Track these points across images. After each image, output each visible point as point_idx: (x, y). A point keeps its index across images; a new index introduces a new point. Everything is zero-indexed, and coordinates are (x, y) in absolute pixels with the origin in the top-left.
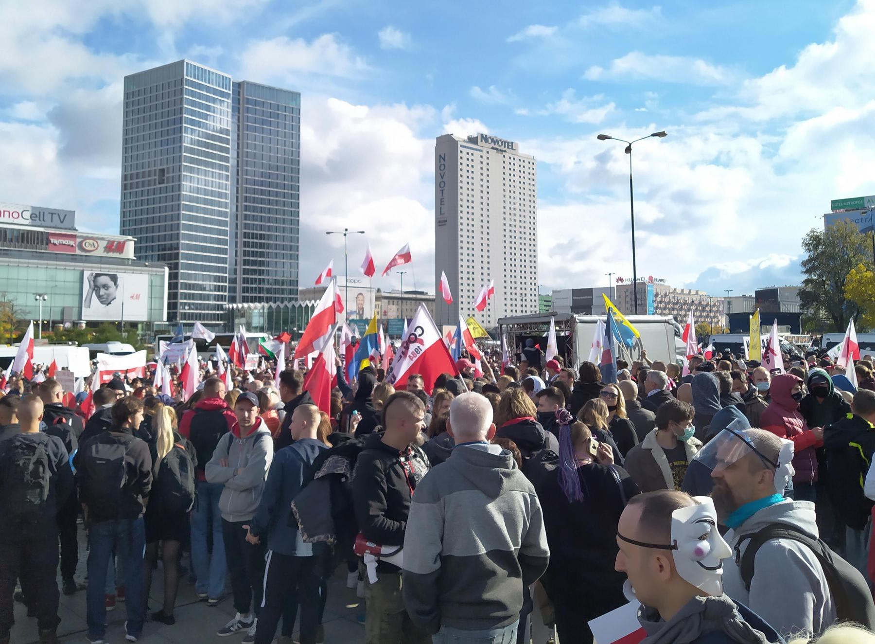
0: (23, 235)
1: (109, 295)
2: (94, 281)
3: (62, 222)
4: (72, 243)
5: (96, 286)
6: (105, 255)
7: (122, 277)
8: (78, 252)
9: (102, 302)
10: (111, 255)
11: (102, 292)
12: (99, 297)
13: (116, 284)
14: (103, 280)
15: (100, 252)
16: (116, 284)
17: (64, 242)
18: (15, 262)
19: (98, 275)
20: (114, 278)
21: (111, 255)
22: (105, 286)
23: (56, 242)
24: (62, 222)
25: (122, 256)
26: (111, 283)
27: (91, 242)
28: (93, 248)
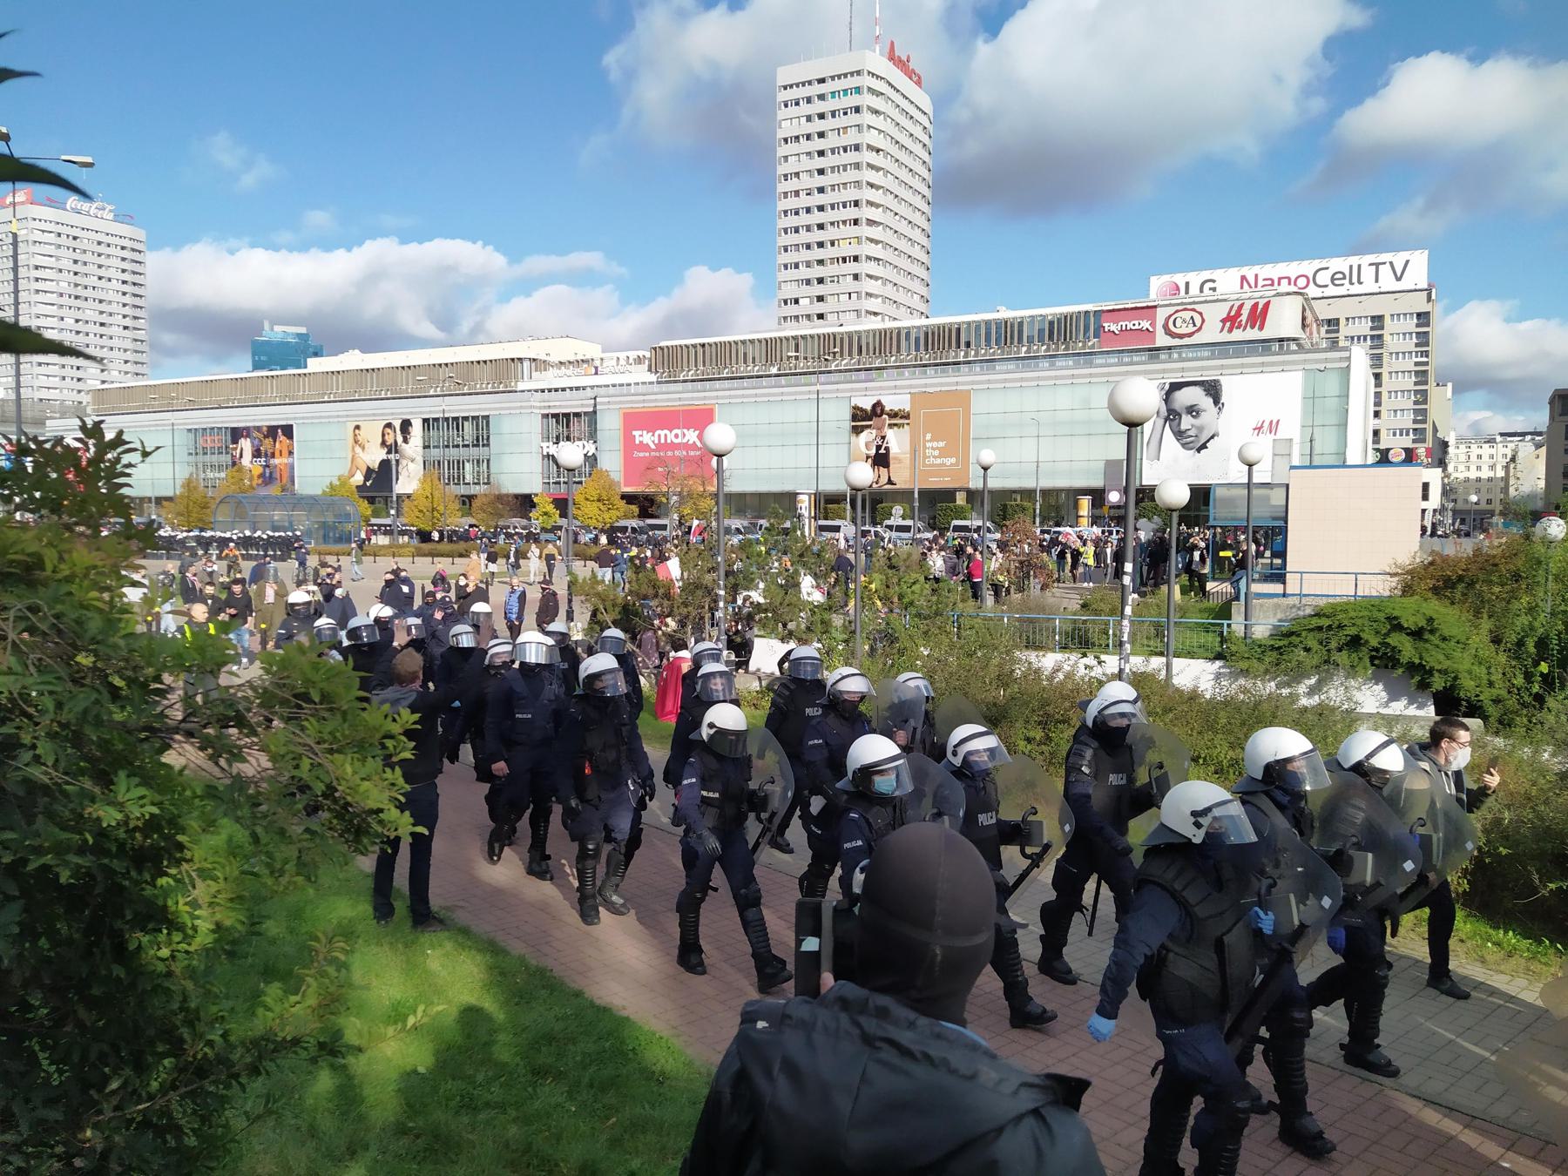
0: (1051, 323)
1: (1200, 429)
2: (1166, 401)
3: (1398, 279)
4: (1146, 324)
5: (1171, 411)
6: (1226, 337)
7: (1231, 386)
8: (1162, 340)
9: (1184, 445)
10: (1238, 335)
11: (1186, 422)
12: (1179, 434)
13: (1216, 401)
14: (1184, 397)
15: (1213, 332)
16: (1216, 401)
17: (1130, 326)
18: (1032, 379)
19: (1176, 387)
20: (1213, 390)
21: (1238, 335)
22: (1193, 410)
23: (1113, 328)
24: (1398, 279)
25: (1267, 333)
26: (1206, 402)
27: (1187, 315)
28: (1191, 329)
